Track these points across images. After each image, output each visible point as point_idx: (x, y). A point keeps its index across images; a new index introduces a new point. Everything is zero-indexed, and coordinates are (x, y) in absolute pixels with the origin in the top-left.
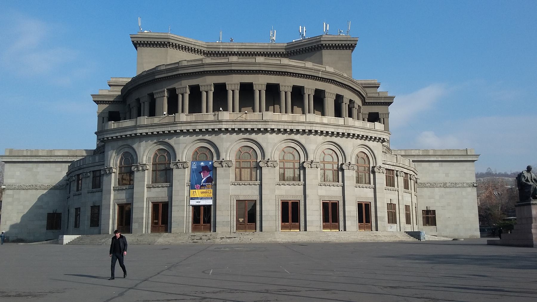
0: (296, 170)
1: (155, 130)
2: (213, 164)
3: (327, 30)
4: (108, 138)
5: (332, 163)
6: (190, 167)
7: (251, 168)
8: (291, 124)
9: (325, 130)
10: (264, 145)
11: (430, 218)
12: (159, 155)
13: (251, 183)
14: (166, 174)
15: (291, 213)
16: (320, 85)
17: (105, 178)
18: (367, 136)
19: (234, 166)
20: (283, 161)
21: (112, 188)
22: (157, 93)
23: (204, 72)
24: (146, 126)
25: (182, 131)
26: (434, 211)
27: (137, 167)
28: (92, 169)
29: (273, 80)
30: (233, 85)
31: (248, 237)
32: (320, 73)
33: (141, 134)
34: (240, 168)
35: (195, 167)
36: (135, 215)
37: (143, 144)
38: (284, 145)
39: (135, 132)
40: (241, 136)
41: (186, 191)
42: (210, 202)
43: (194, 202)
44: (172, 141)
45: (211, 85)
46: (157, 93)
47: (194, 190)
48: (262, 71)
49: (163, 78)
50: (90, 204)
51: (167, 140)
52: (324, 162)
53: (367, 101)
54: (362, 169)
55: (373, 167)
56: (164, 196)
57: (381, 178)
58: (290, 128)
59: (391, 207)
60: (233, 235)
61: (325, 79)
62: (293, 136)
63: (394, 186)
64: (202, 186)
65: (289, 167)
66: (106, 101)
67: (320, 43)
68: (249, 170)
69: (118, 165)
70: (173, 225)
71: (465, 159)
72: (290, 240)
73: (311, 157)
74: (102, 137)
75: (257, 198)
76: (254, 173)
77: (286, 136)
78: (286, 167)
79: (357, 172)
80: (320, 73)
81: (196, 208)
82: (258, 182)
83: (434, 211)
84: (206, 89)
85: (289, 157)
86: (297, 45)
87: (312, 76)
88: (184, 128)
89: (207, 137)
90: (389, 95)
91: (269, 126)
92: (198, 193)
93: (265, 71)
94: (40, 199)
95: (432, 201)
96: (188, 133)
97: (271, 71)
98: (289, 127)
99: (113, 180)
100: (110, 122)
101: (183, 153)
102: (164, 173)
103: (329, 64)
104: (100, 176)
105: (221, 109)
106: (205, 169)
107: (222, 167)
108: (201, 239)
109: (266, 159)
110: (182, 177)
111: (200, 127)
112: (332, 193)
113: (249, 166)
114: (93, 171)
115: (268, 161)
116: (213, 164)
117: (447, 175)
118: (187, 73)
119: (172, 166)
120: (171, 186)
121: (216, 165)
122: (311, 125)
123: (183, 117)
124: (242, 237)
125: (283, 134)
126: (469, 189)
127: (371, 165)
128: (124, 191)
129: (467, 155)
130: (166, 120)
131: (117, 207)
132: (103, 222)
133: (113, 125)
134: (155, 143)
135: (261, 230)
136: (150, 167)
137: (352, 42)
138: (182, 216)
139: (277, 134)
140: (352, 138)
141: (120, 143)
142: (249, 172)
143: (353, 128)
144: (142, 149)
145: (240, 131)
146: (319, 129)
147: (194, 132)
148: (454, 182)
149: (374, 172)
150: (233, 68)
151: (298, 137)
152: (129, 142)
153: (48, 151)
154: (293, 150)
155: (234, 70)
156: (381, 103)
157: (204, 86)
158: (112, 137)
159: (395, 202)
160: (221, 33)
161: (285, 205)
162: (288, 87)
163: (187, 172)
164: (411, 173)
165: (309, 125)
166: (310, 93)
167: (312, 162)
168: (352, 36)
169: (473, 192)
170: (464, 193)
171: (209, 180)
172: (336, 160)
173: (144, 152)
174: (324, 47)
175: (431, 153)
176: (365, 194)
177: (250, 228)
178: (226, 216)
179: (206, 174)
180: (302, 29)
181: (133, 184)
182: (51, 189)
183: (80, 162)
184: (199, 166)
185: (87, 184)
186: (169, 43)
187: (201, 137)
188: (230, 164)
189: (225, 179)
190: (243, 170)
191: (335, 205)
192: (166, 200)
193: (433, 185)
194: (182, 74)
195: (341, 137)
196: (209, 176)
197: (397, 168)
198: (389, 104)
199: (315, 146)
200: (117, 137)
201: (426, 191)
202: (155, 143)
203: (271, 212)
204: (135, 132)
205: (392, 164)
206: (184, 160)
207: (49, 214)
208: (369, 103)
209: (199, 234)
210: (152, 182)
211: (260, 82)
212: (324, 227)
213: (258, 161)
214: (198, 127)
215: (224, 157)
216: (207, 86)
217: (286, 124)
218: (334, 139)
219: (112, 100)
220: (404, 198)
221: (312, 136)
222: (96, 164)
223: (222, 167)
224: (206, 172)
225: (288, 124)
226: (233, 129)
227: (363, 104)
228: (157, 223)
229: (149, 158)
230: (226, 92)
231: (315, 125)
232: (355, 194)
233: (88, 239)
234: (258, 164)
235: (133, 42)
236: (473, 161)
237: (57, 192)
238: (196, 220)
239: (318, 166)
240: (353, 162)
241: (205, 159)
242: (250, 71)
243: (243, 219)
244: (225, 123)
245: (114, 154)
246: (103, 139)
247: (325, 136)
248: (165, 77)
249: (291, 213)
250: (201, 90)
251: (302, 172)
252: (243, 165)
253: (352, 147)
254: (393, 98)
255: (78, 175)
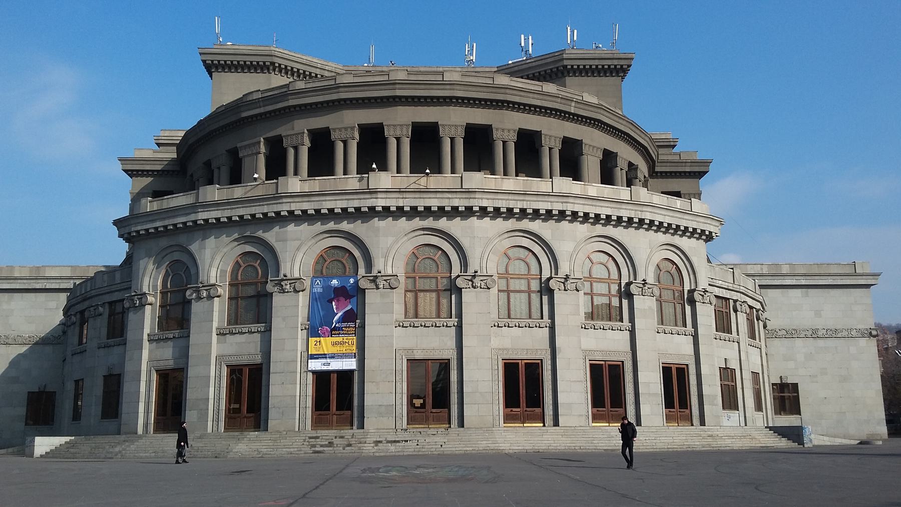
0: (533, 296)
1: (236, 213)
2: (356, 282)
3: (572, 40)
4: (138, 232)
5: (608, 281)
6: (308, 291)
7: (437, 291)
8: (521, 198)
9: (592, 210)
10: (465, 242)
11: (787, 397)
12: (243, 266)
13: (439, 322)
14: (258, 305)
15: (525, 388)
16: (573, 130)
17: (132, 317)
18: (678, 227)
20: (506, 275)
21: (145, 337)
22: (245, 147)
23: (339, 101)
24: (217, 205)
25: (291, 213)
26: (795, 386)
27: (197, 290)
28: (108, 298)
29: (479, 116)
30: (398, 128)
31: (436, 439)
32: (573, 104)
33: (206, 221)
34: (416, 292)
35: (320, 290)
36: (191, 394)
37: (211, 242)
39: (193, 217)
40: (417, 222)
41: (299, 341)
42: (350, 364)
43: (316, 365)
44: (271, 236)
45: (353, 128)
46: (245, 147)
47: (318, 339)
48: (457, 98)
49: (256, 116)
50: (102, 372)
51: (260, 234)
52: (590, 279)
53: (657, 169)
54: (668, 295)
55: (691, 292)
56: (253, 351)
57: (706, 315)
58: (520, 205)
59: (727, 373)
60: (401, 436)
61: (582, 117)
62: (526, 224)
63: (729, 331)
64: (335, 329)
65: (517, 289)
66: (148, 171)
67: (560, 64)
68: (434, 295)
69: (159, 288)
70: (272, 413)
71: (854, 282)
72: (529, 447)
73: (564, 269)
74: (127, 230)
75: (450, 353)
76: (444, 302)
77: (512, 224)
78: (512, 288)
79: (660, 301)
80: (573, 104)
81: (322, 378)
82: (454, 320)
83: (795, 386)
84: (343, 136)
85: (518, 268)
86: (516, 68)
87: (556, 110)
88: (297, 207)
89: (345, 226)
90: (699, 157)
91: (477, 203)
92: (326, 344)
93: (463, 99)
94: (14, 363)
95: (791, 365)
96: (305, 217)
97: (474, 99)
98: (517, 206)
99: (149, 319)
100: (143, 201)
101: (293, 261)
102: (253, 303)
103: (584, 94)
104: (124, 312)
105: (374, 166)
106: (341, 293)
107: (378, 288)
108: (331, 444)
109: (471, 271)
110: (292, 311)
111: (330, 205)
112: (610, 343)
113: (434, 287)
114: (110, 303)
115: (474, 277)
116: (356, 282)
117: (818, 313)
118: (305, 105)
119: (270, 287)
120: (269, 330)
121: (363, 284)
122: (565, 200)
123: (294, 184)
124: (422, 440)
125: (506, 219)
126: (863, 342)
127: (687, 288)
128: (170, 343)
129: (855, 274)
130: (259, 192)
131: (154, 376)
132: (125, 408)
133: (149, 205)
134: (235, 240)
135: (461, 424)
136: (224, 291)
137: (622, 62)
138: (290, 393)
139: (493, 218)
140: (647, 230)
141: (164, 242)
142: (434, 300)
143: (649, 209)
144: (208, 253)
145: (414, 212)
146: (581, 209)
147: (318, 216)
148: (833, 328)
149: (692, 302)
150: (399, 93)
151: (536, 226)
152: (182, 239)
153: (31, 269)
154: (527, 252)
155: (400, 97)
156: (685, 172)
157: (340, 129)
158: (147, 230)
159: (734, 364)
160: (372, 49)
161: (510, 369)
162: (509, 131)
163: (303, 299)
164: (758, 306)
165: (561, 199)
166: (552, 144)
167: (567, 278)
168: (621, 50)
169: (869, 349)
170: (853, 350)
171: (349, 317)
172: (614, 275)
173: (213, 259)
174: (569, 73)
175: (785, 270)
176: (679, 348)
177: (438, 421)
178: (385, 395)
179: (342, 304)
180: (526, 40)
181: (188, 328)
182: (37, 343)
183: (86, 286)
184: (327, 288)
185: (97, 329)
186: (273, 64)
187: (331, 225)
188: (394, 283)
189: (384, 313)
190: (421, 295)
191: (616, 370)
192: (258, 359)
193: (791, 334)
194: (294, 107)
195: (626, 227)
196: (349, 308)
198: (701, 174)
199: (573, 244)
200: (156, 228)
201: (779, 346)
202: (235, 240)
203: (482, 386)
204: (193, 217)
205: (725, 285)
206: (297, 275)
207: (31, 394)
208: (661, 172)
209: (327, 434)
210: (229, 323)
211: (453, 121)
212: (596, 418)
213: (454, 275)
214: (326, 205)
215: (381, 268)
216: (346, 129)
217: (511, 197)
218: (610, 231)
219: (159, 168)
220: (752, 359)
221: (564, 224)
222: (114, 288)
223: (378, 288)
224: (342, 299)
225: (517, 197)
226: (400, 209)
227: (651, 176)
228: (238, 411)
229: (223, 272)
230: (384, 141)
231: (571, 200)
232: (658, 346)
233: (87, 445)
234: (452, 282)
235: (204, 61)
236: (868, 286)
237: (48, 349)
238: (321, 403)
239: (579, 285)
240: (651, 280)
241: (340, 272)
242: (432, 98)
243: (422, 401)
244: (383, 195)
245: (151, 266)
246: (129, 233)
247: (593, 224)
248: (261, 114)
249: (525, 388)
250: (333, 137)
251: (545, 299)
252: (420, 284)
253: (647, 249)
254: (707, 163)
255: (82, 312)
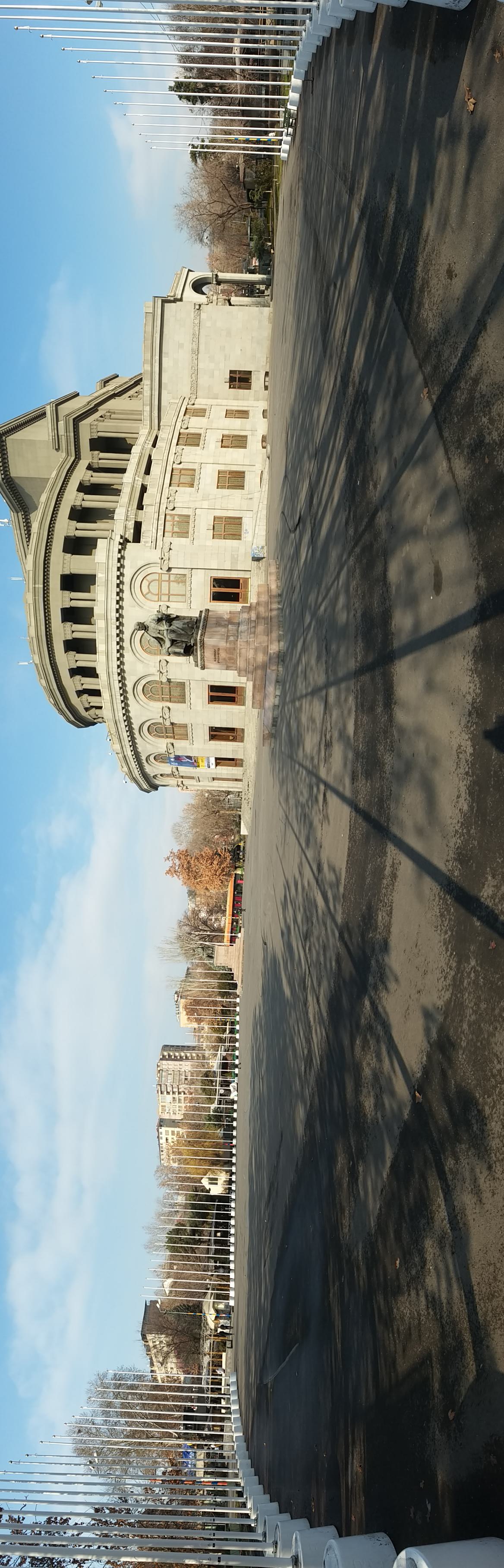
19: (172, 740)
38: (142, 696)
77: (130, 695)
127: (160, 571)
161: (212, 699)
197: (163, 507)
